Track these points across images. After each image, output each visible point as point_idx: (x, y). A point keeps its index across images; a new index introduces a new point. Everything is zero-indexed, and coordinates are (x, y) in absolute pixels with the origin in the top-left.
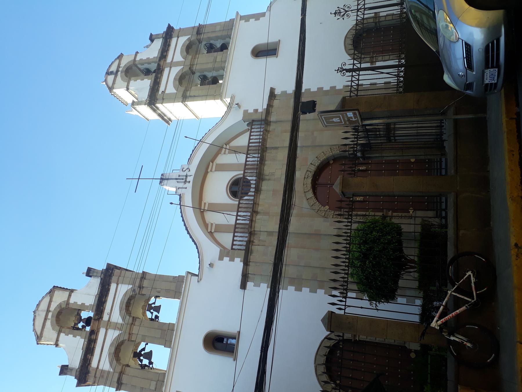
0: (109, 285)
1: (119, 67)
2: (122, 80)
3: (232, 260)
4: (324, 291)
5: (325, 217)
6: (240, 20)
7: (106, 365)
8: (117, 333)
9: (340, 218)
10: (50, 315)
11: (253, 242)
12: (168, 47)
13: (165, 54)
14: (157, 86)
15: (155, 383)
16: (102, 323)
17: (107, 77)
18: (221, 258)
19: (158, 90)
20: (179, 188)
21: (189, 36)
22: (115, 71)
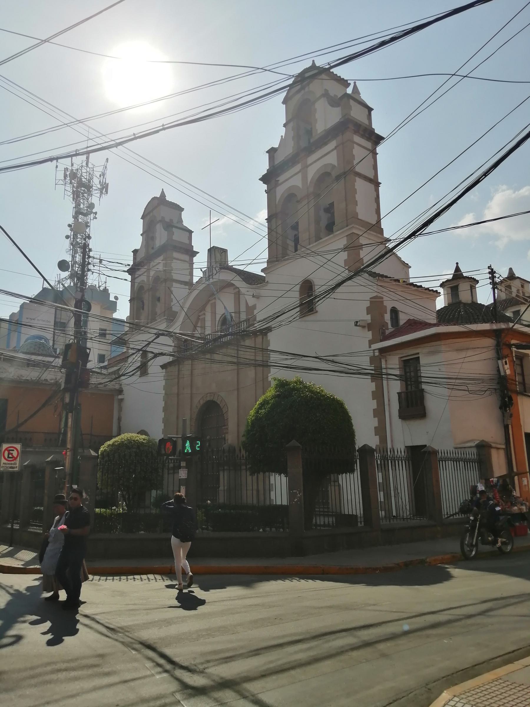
6: (347, 236)
8: (146, 280)
10: (151, 214)
13: (313, 149)
19: (278, 175)
20: (206, 273)
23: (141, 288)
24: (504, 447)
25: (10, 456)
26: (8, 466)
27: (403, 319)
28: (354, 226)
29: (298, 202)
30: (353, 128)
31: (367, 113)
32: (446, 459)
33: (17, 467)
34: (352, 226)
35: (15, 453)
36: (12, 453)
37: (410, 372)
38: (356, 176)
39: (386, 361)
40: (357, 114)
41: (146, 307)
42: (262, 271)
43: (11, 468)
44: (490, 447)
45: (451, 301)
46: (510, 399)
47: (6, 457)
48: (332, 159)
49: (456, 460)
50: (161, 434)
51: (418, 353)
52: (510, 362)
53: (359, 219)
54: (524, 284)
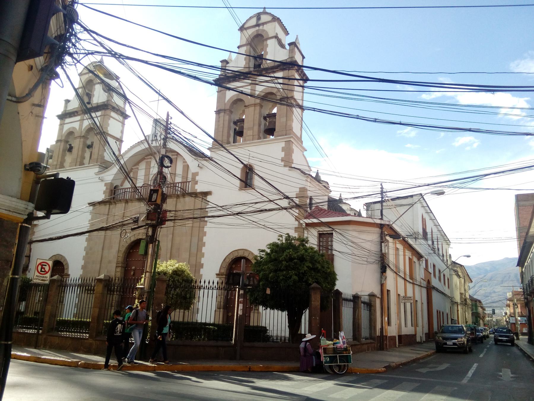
0: (100, 110)
1: (263, 24)
3: (104, 192)
4: (85, 255)
5: (119, 251)
6: (285, 141)
7: (66, 128)
8: (78, 129)
9: (117, 262)
11: (112, 204)
12: (271, 72)
15: (56, 164)
16: (82, 116)
18: (106, 185)
19: (230, 82)
22: (260, 22)
23: (71, 133)
25: (43, 270)
26: (40, 278)
28: (293, 136)
29: (245, 106)
33: (47, 280)
35: (47, 268)
36: (45, 268)
37: (323, 242)
41: (75, 150)
42: (209, 149)
43: (42, 280)
47: (39, 271)
50: (82, 259)
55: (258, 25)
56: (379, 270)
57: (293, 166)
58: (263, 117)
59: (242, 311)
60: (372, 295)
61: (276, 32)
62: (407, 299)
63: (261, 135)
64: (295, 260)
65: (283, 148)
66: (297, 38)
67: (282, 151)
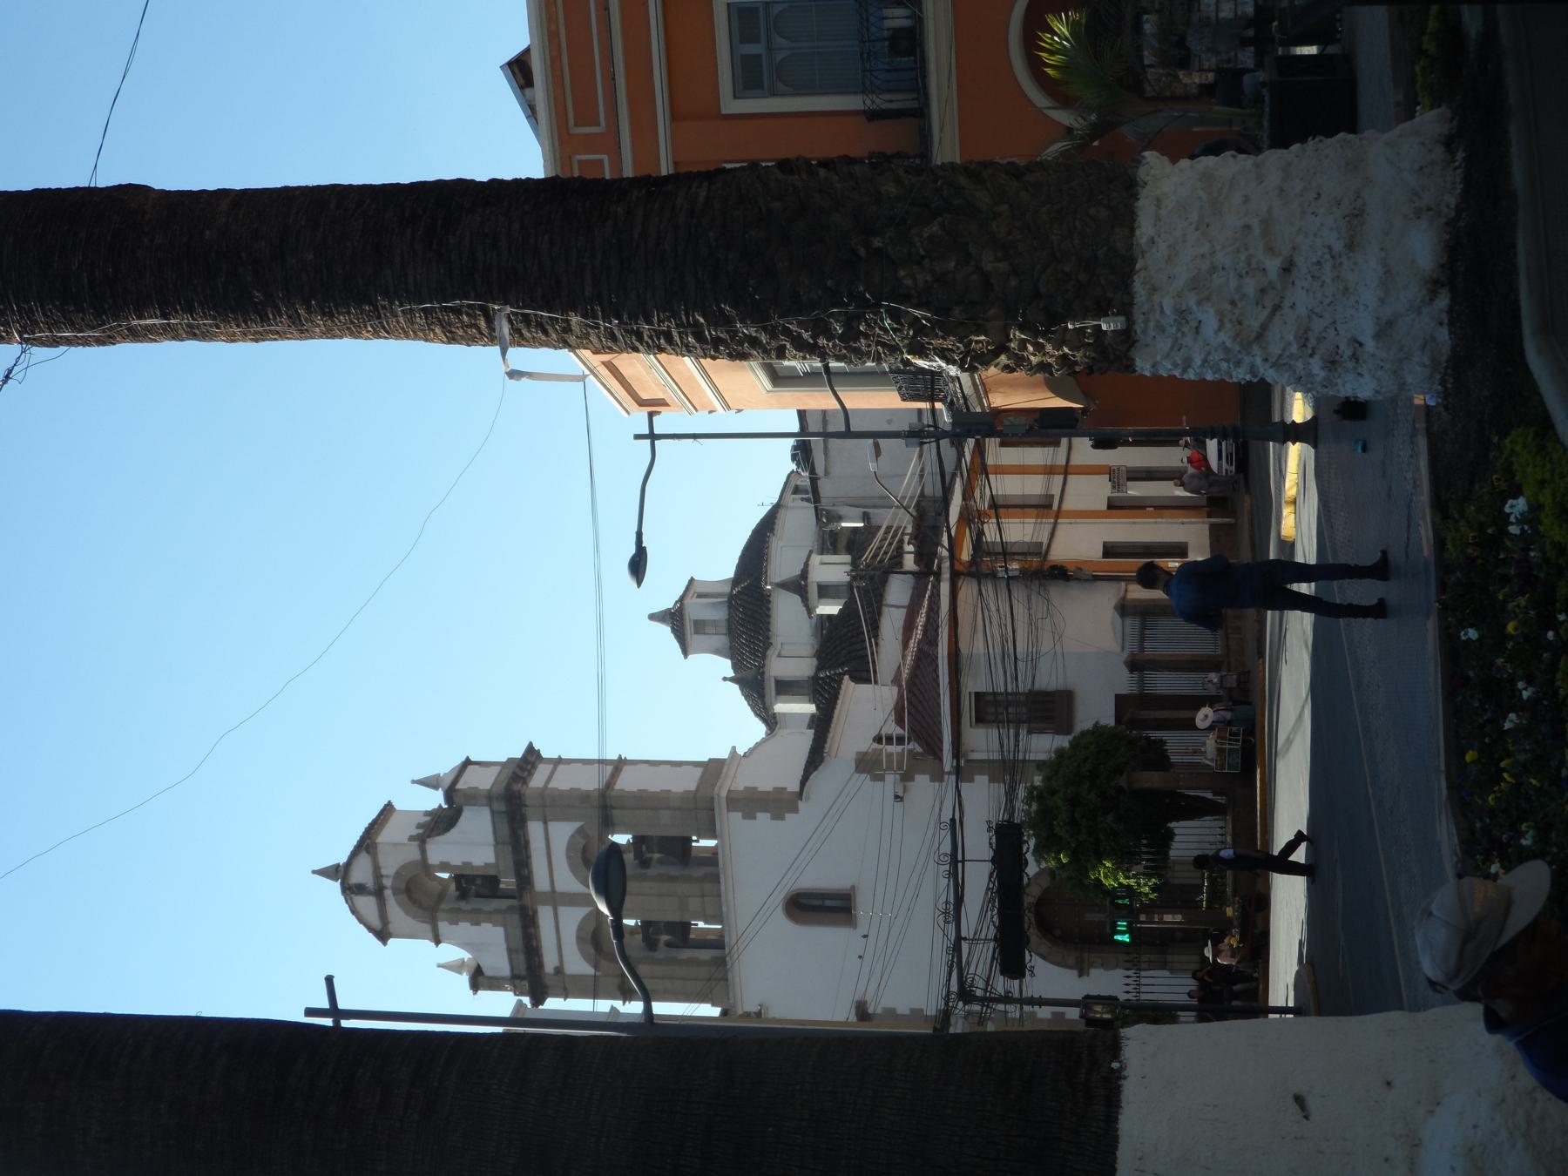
1: (378, 875)
2: (407, 913)
6: (728, 811)
14: (536, 959)
17: (351, 899)
19: (541, 965)
21: (582, 823)
24: (1123, 584)
27: (893, 729)
30: (520, 785)
31: (476, 767)
32: (1142, 649)
34: (716, 797)
38: (613, 789)
39: (972, 751)
40: (482, 781)
44: (1124, 598)
45: (807, 698)
46: (1054, 567)
48: (564, 832)
49: (1142, 638)
51: (970, 693)
52: (996, 563)
53: (698, 787)
54: (695, 593)
55: (379, 893)
56: (1062, 582)
57: (794, 786)
58: (644, 871)
59: (1175, 916)
60: (1124, 608)
61: (406, 841)
62: (1118, 479)
63: (699, 872)
64: (1076, 815)
65: (745, 817)
66: (425, 782)
67: (755, 818)
